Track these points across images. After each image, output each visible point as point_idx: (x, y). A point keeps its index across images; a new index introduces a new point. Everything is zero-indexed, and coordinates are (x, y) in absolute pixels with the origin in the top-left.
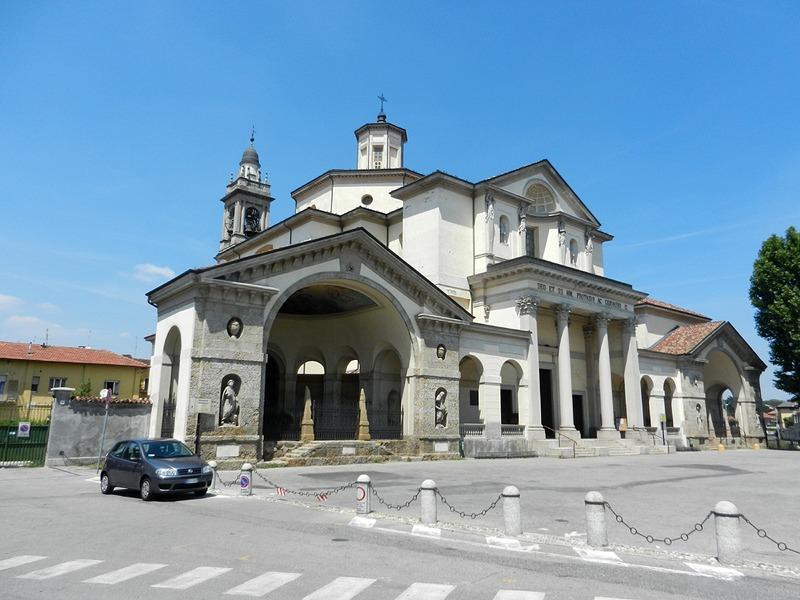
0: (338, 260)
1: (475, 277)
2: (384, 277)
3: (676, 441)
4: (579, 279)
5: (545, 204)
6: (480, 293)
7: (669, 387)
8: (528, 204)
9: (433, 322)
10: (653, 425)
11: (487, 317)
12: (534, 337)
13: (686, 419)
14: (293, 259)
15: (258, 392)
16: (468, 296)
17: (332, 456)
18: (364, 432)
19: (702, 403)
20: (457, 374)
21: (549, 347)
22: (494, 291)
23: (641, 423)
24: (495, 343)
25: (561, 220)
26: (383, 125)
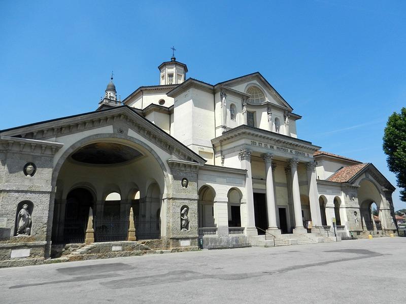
0: (112, 126)
1: (216, 138)
2: (145, 137)
3: (342, 233)
4: (277, 138)
6: (219, 149)
7: (337, 201)
8: (248, 97)
9: (179, 164)
10: (328, 224)
11: (223, 163)
12: (249, 173)
13: (348, 221)
14: (77, 125)
15: (47, 212)
16: (212, 151)
17: (105, 253)
18: (131, 235)
19: (358, 211)
20: (195, 196)
21: (259, 179)
22: (225, 147)
23: (320, 224)
24: (224, 177)
25: (269, 107)
26: (174, 62)
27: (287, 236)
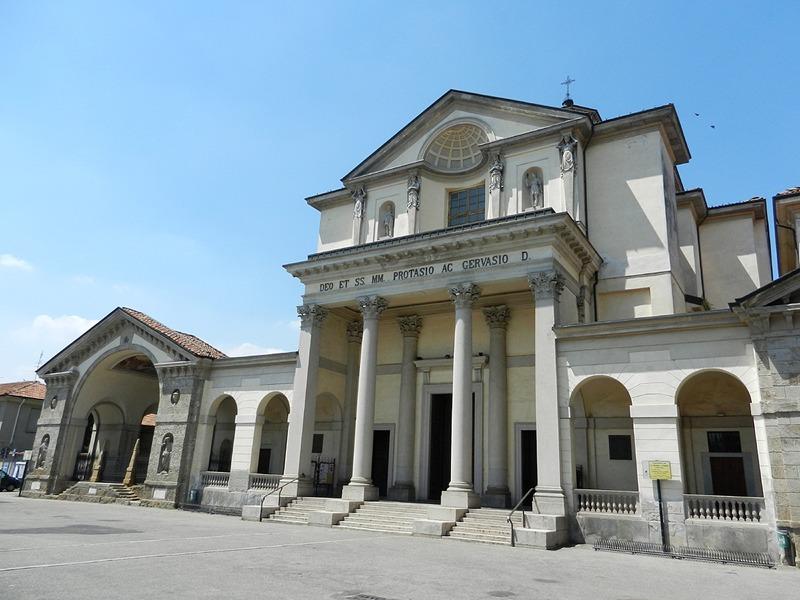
4: (377, 254)
5: (451, 148)
12: (305, 359)
24: (256, 376)
27: (386, 506)
